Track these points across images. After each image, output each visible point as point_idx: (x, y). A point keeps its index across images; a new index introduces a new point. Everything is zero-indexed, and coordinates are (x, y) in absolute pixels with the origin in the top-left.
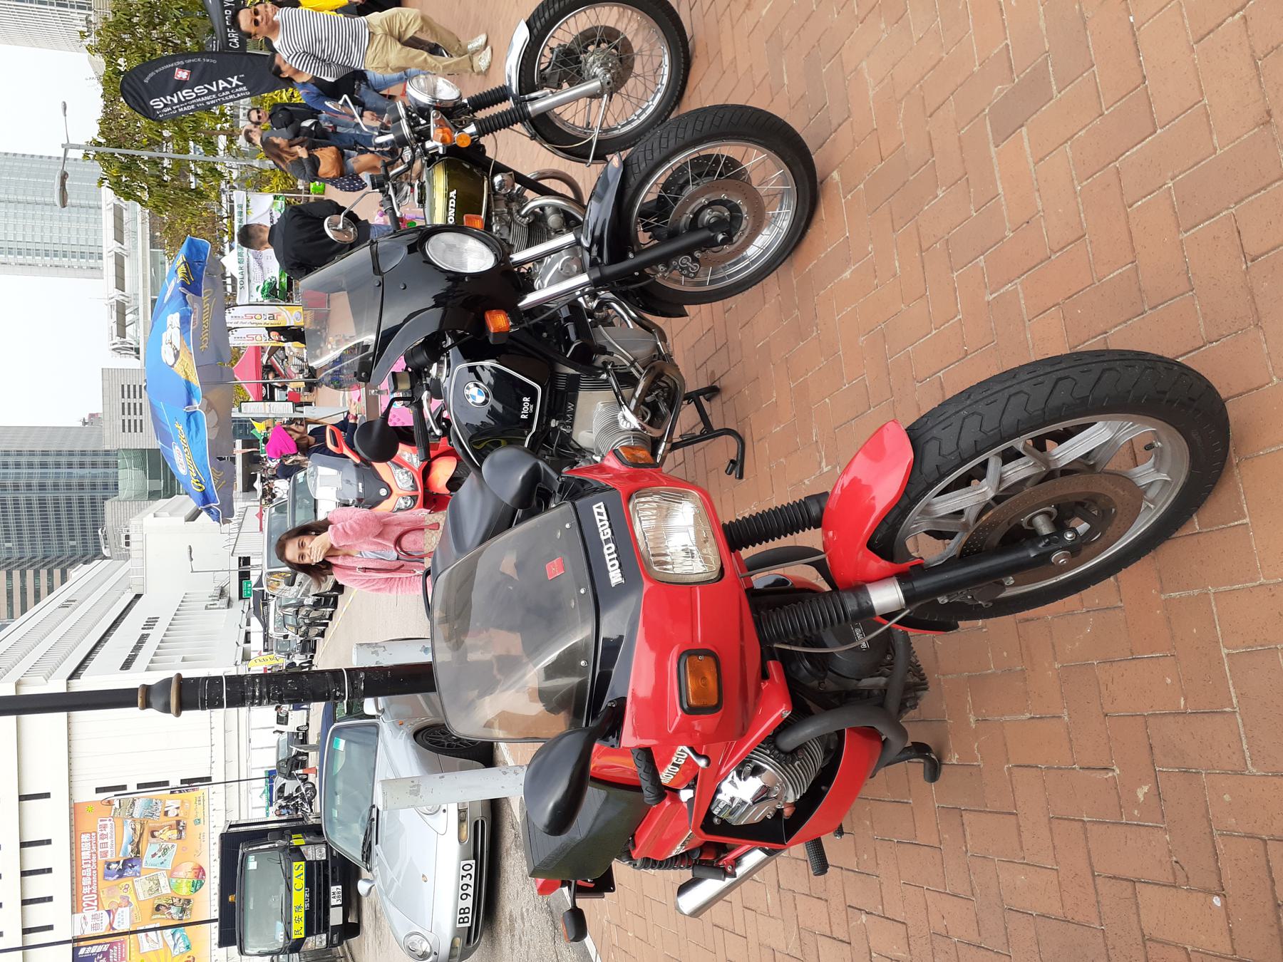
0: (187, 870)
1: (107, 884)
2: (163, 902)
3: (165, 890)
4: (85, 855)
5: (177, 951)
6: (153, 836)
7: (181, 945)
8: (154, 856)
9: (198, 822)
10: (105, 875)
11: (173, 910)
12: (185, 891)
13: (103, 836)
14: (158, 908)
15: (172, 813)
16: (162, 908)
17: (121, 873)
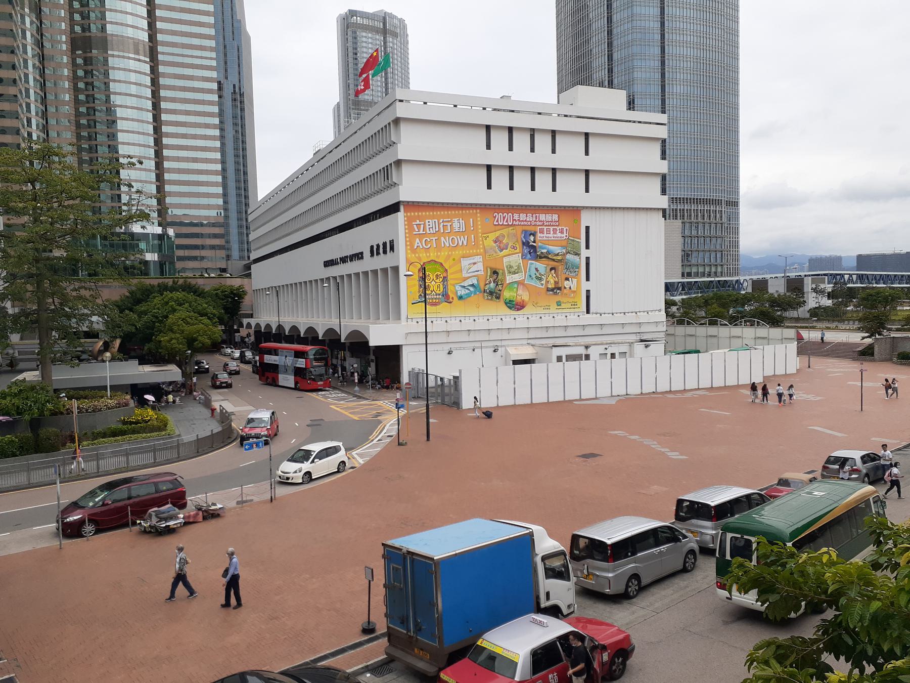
0: (523, 295)
1: (519, 233)
2: (500, 277)
3: (509, 279)
4: (542, 217)
5: (458, 288)
6: (551, 269)
7: (463, 292)
8: (537, 269)
9: (559, 304)
10: (526, 231)
11: (492, 285)
12: (507, 294)
13: (555, 231)
14: (495, 272)
15: (566, 283)
16: (495, 276)
17: (526, 244)
